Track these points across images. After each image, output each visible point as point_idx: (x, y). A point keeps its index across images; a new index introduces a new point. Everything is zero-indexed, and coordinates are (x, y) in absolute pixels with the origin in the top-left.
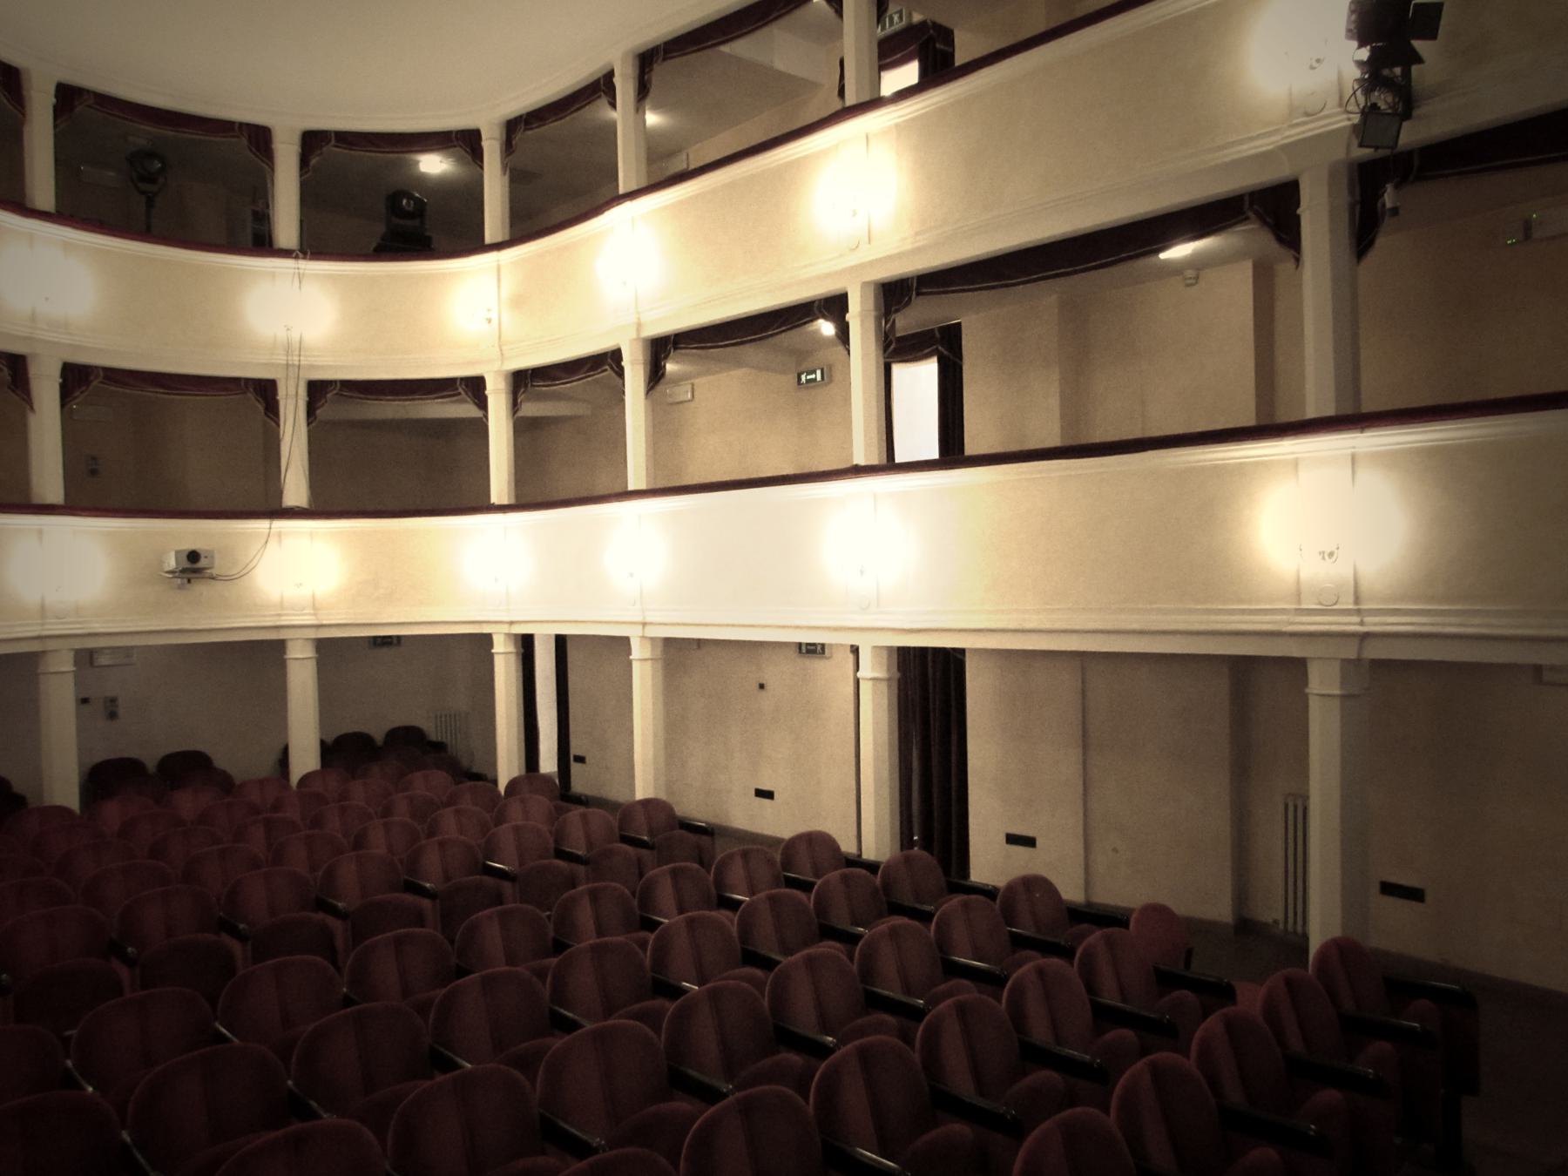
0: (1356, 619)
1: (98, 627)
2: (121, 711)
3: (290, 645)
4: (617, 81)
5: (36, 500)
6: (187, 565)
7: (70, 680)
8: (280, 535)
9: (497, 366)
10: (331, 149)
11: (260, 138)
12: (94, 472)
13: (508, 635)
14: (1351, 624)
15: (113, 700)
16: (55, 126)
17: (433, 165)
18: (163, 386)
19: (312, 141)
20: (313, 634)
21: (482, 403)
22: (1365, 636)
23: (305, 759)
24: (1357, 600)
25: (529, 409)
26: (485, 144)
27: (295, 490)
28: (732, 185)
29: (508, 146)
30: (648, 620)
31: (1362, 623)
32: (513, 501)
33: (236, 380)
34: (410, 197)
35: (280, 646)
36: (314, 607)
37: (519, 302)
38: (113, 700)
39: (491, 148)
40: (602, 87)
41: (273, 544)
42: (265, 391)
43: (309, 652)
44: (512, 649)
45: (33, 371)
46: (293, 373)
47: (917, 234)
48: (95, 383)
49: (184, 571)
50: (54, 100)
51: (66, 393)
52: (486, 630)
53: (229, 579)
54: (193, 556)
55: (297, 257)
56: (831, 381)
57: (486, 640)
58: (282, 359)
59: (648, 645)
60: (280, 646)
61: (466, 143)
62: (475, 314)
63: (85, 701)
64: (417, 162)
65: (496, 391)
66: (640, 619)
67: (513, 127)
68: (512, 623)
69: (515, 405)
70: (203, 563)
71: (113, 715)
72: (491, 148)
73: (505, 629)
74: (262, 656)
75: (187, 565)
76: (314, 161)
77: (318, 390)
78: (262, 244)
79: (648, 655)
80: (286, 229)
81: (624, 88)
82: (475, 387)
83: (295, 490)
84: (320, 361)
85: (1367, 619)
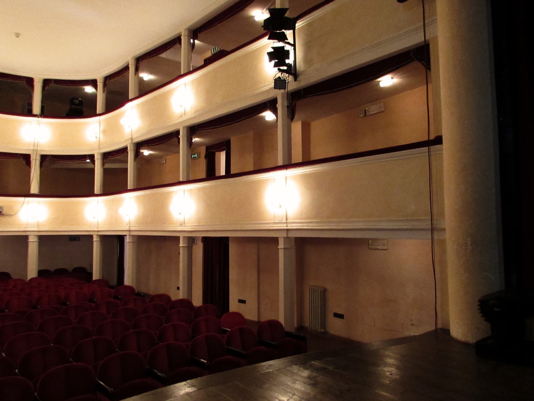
0: (286, 225)
3: (29, 237)
4: (130, 66)
8: (28, 202)
9: (97, 151)
11: (30, 81)
14: (284, 227)
17: (89, 89)
19: (46, 82)
21: (93, 162)
22: (288, 230)
23: (32, 272)
24: (287, 219)
25: (107, 166)
26: (98, 84)
27: (34, 188)
28: (155, 97)
29: (105, 85)
30: (131, 229)
31: (287, 226)
32: (102, 193)
34: (77, 99)
35: (26, 238)
36: (38, 225)
37: (105, 132)
39: (100, 85)
40: (126, 69)
41: (25, 206)
42: (26, 158)
43: (36, 239)
44: (99, 240)
46: (35, 152)
47: (195, 112)
52: (91, 233)
55: (38, 117)
56: (200, 157)
57: (91, 236)
58: (32, 148)
59: (131, 237)
60: (26, 238)
61: (93, 83)
62: (91, 135)
64: (84, 89)
65: (97, 159)
66: (128, 229)
67: (107, 79)
68: (98, 231)
69: (103, 164)
72: (100, 85)
73: (96, 233)
74: (21, 240)
77: (44, 158)
78: (29, 113)
79: (131, 241)
80: (37, 108)
81: (132, 69)
82: (92, 157)
83: (34, 188)
85: (289, 225)
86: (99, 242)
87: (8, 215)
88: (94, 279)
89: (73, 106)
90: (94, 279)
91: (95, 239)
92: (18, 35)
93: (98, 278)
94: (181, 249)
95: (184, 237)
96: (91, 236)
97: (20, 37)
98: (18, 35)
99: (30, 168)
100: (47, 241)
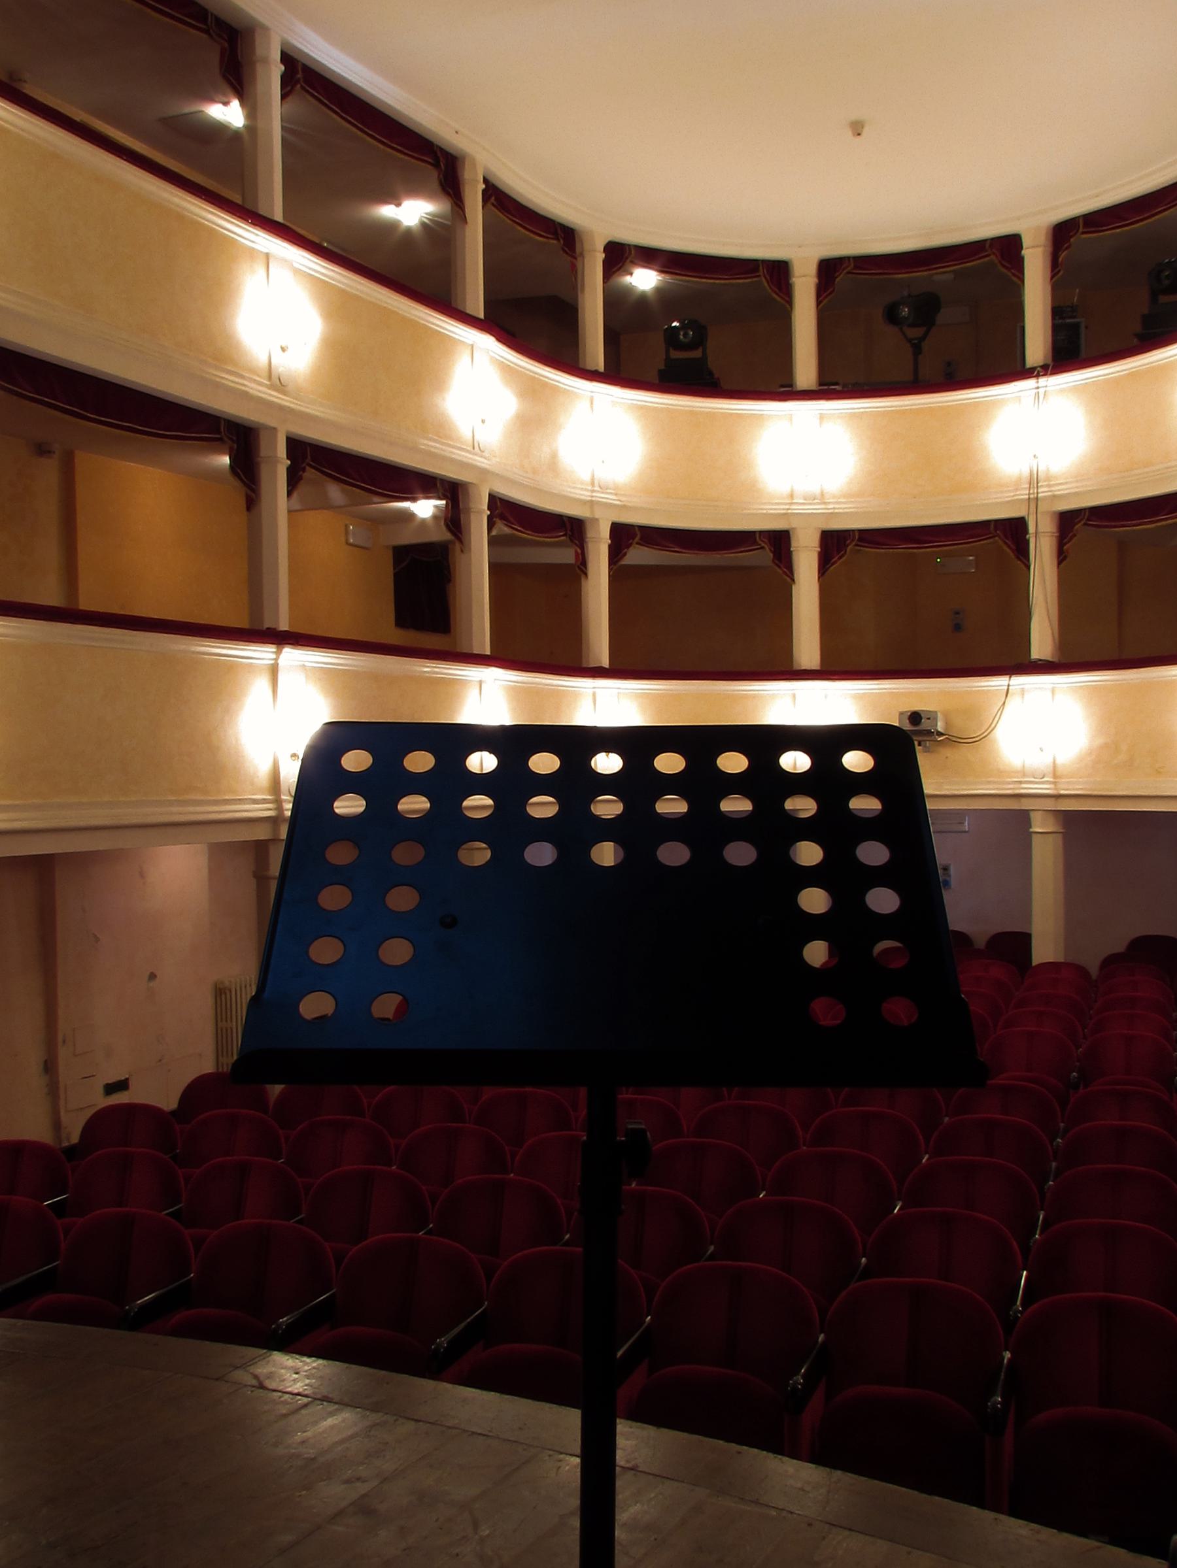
3: (1032, 814)
5: (796, 667)
8: (1023, 692)
10: (1081, 238)
12: (958, 628)
16: (818, 303)
20: (1051, 805)
33: (986, 524)
35: (1023, 817)
36: (1055, 775)
41: (1013, 704)
42: (1012, 533)
46: (1033, 509)
55: (1038, 376)
58: (1023, 494)
60: (1023, 817)
70: (925, 724)
76: (1063, 256)
77: (1069, 523)
84: (1060, 490)
87: (953, 740)
89: (1163, 299)
92: (857, 129)
97: (866, 131)
98: (857, 129)
99: (1028, 567)
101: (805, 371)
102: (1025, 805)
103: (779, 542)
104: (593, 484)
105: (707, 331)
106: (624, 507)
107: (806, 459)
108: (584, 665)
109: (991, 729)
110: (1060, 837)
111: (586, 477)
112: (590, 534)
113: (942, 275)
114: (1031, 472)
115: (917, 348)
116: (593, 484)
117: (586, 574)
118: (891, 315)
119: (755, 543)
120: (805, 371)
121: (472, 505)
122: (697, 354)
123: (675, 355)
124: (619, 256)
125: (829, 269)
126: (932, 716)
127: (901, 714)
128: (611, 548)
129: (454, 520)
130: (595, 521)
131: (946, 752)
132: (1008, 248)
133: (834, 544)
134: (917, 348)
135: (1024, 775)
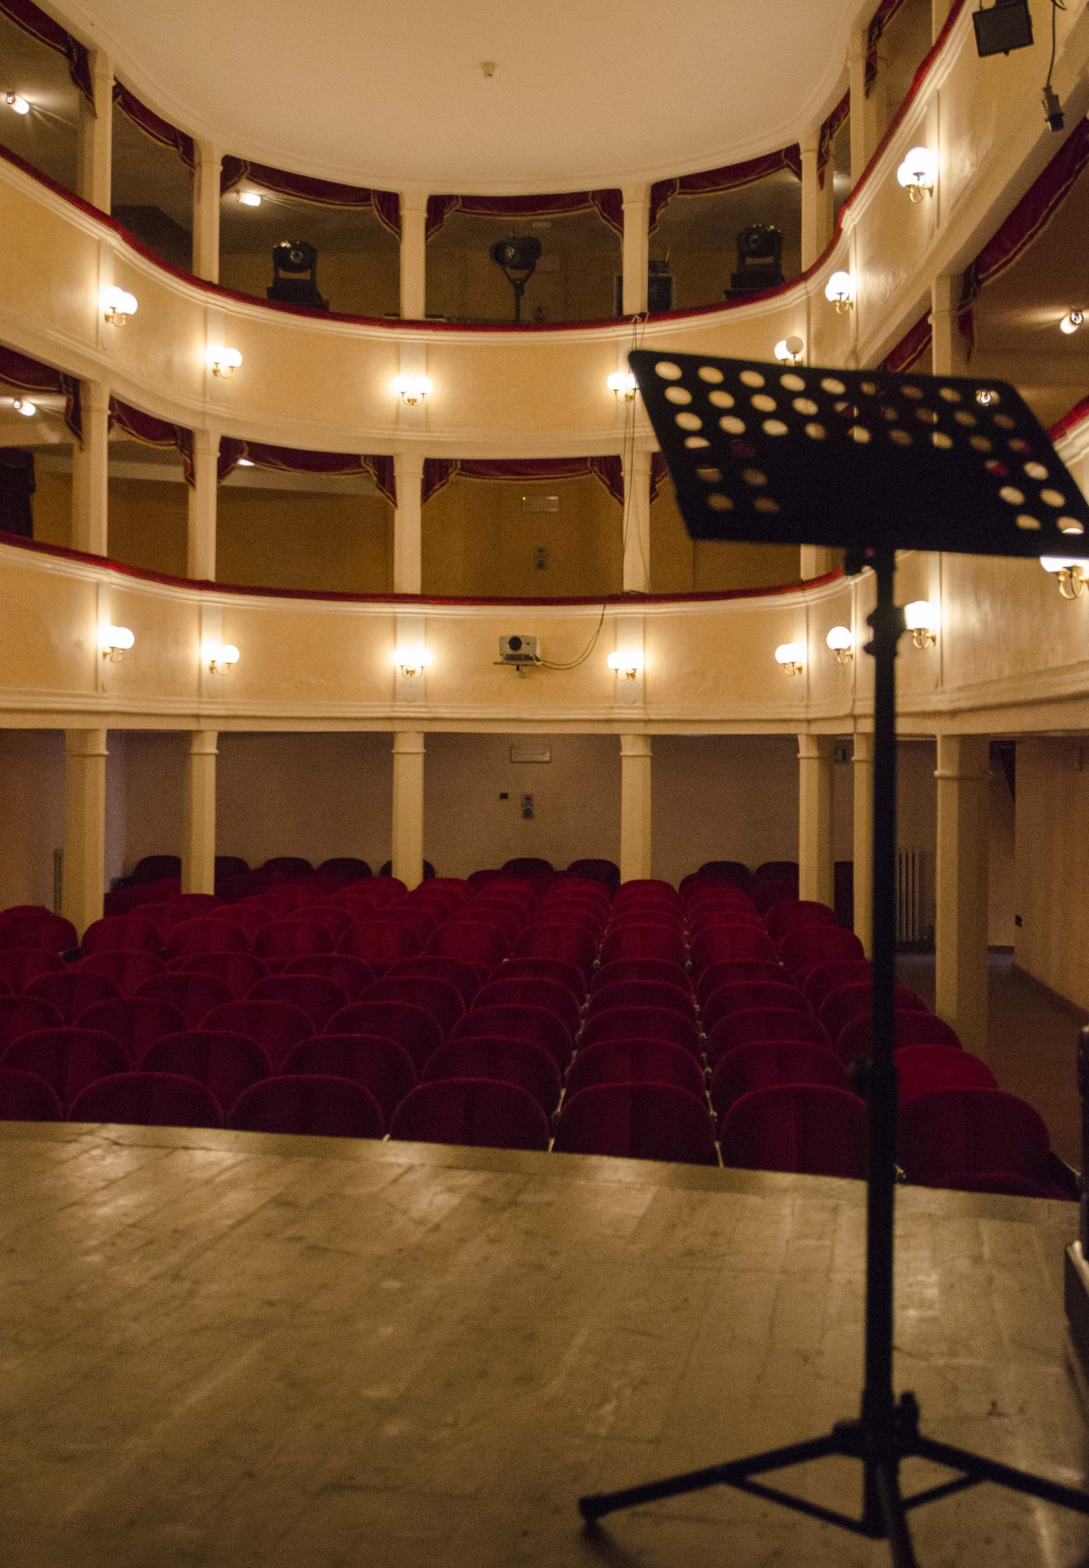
1: (443, 712)
2: (536, 811)
3: (623, 739)
6: (510, 651)
7: (420, 760)
8: (616, 622)
10: (676, 197)
12: (541, 565)
13: (809, 736)
15: (528, 798)
16: (427, 237)
18: (517, 473)
19: (660, 192)
20: (642, 729)
33: (582, 460)
35: (614, 741)
38: (528, 798)
39: (809, 159)
44: (814, 753)
45: (398, 470)
46: (628, 448)
48: (452, 476)
49: (510, 658)
50: (425, 215)
51: (427, 489)
53: (567, 668)
54: (515, 643)
57: (791, 741)
58: (620, 433)
61: (790, 156)
63: (504, 796)
66: (846, 710)
68: (809, 721)
70: (524, 650)
71: (528, 814)
75: (510, 651)
86: (815, 764)
88: (803, 896)
89: (749, 261)
90: (803, 896)
91: (806, 750)
92: (489, 69)
93: (813, 898)
94: (940, 783)
95: (947, 737)
96: (791, 741)
97: (496, 73)
98: (489, 69)
99: (622, 503)
100: (679, 756)
101: (413, 300)
102: (615, 729)
103: (383, 468)
104: (204, 395)
105: (315, 253)
106: (234, 421)
107: (411, 387)
108: (190, 576)
109: (585, 656)
110: (648, 761)
111: (198, 384)
112: (199, 445)
113: (540, 223)
114: (628, 411)
115: (519, 288)
116: (204, 395)
117: (193, 485)
118: (497, 253)
119: (360, 466)
120: (413, 303)
121: (93, 404)
122: (306, 276)
123: (283, 274)
124: (234, 171)
125: (437, 205)
126: (531, 642)
127: (502, 638)
128: (219, 460)
129: (74, 419)
130: (206, 432)
131: (541, 678)
132: (610, 201)
133: (436, 472)
134: (519, 288)
135: (616, 700)
